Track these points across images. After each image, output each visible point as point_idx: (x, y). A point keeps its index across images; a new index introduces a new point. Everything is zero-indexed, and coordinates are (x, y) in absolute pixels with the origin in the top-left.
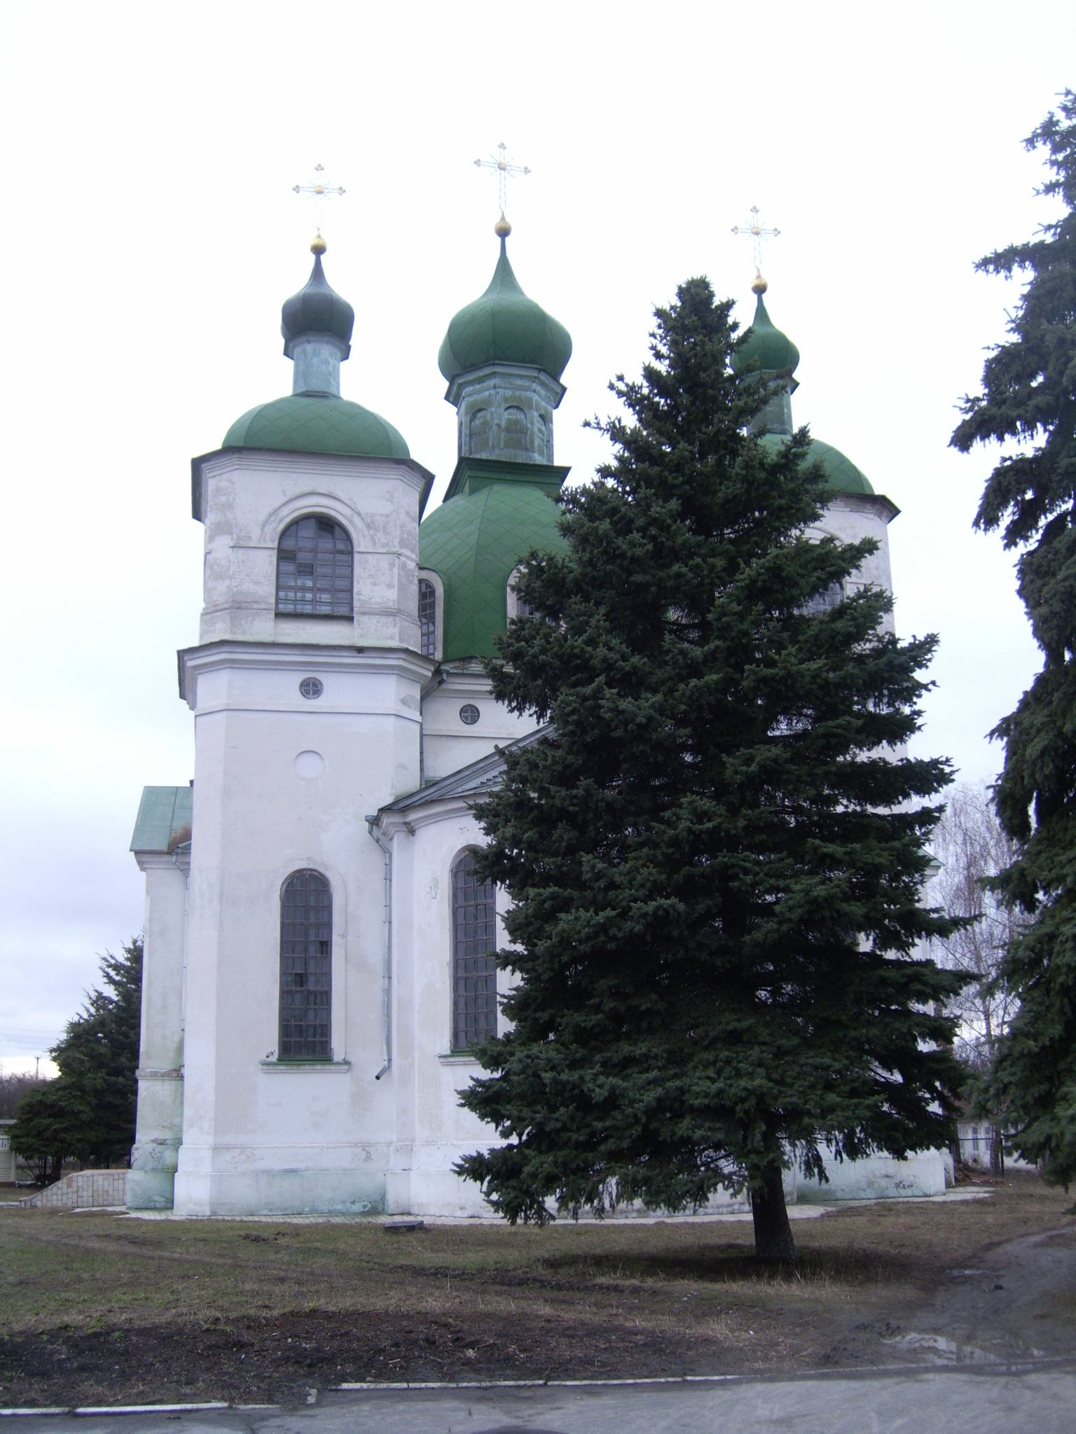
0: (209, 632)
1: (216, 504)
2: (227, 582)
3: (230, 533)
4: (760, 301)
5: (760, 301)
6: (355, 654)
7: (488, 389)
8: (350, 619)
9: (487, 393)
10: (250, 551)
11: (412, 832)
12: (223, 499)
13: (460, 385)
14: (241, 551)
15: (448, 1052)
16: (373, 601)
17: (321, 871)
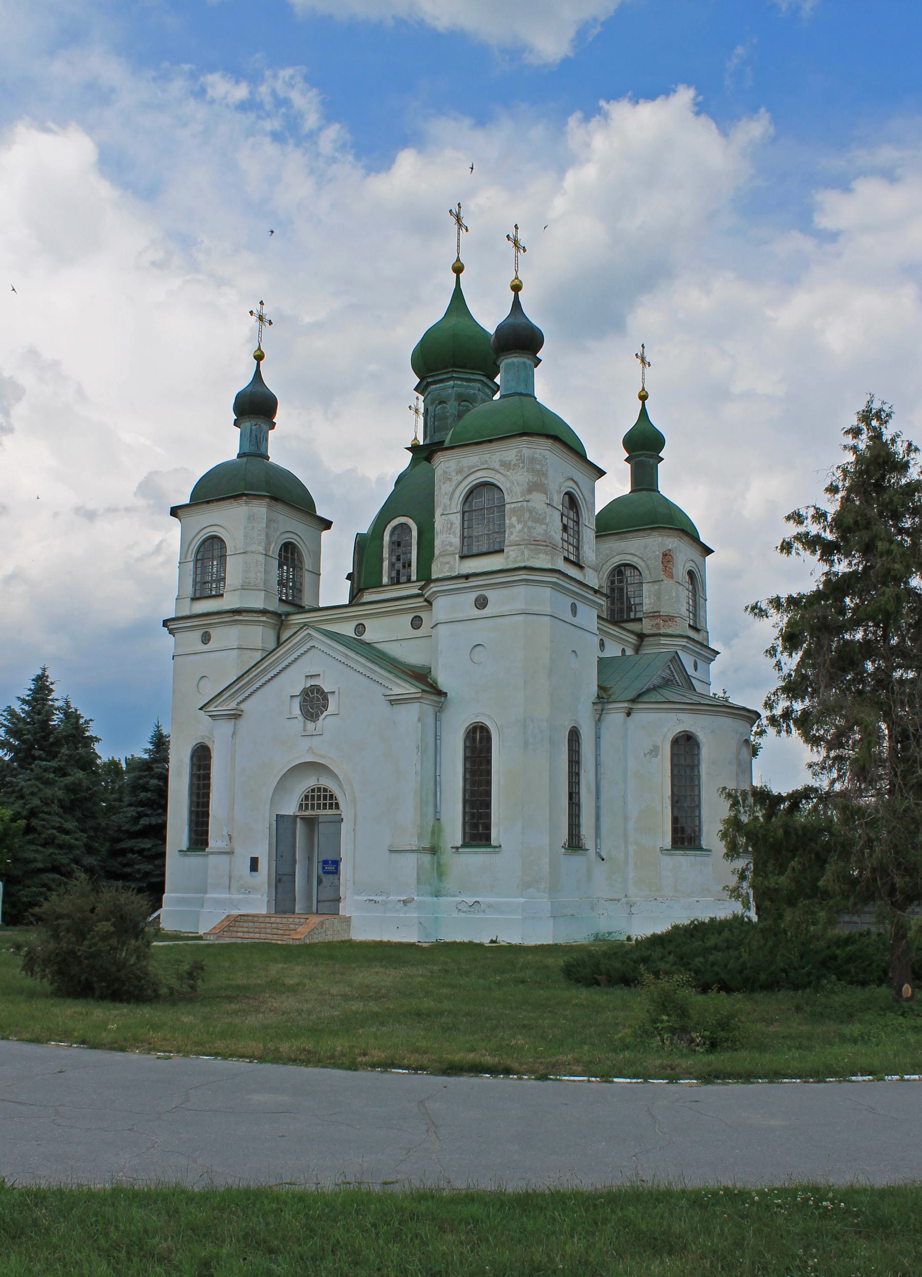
0: (535, 557)
1: (533, 469)
2: (544, 527)
3: (546, 493)
4: (643, 405)
5: (643, 405)
6: (593, 593)
7: (474, 389)
8: (581, 567)
9: (472, 392)
10: (553, 509)
11: (629, 714)
12: (539, 467)
13: (453, 377)
14: (550, 507)
15: (670, 848)
16: (590, 559)
17: (579, 728)
